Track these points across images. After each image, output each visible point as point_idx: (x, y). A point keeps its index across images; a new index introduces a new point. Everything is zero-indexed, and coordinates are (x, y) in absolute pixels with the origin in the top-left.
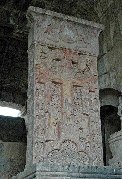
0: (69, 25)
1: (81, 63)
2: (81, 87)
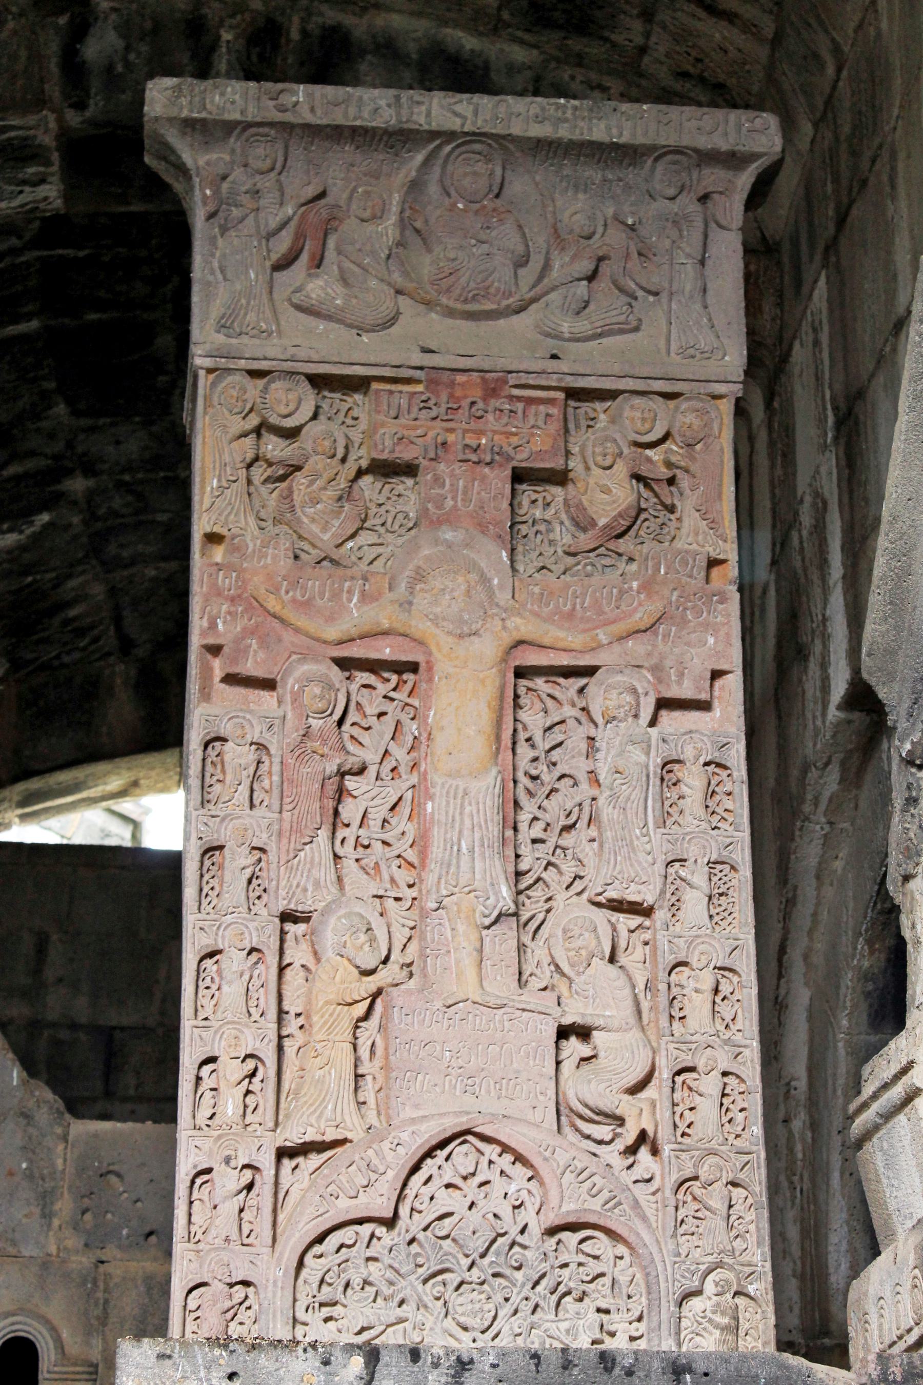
0: (481, 167)
1: (596, 471)
2: (590, 671)
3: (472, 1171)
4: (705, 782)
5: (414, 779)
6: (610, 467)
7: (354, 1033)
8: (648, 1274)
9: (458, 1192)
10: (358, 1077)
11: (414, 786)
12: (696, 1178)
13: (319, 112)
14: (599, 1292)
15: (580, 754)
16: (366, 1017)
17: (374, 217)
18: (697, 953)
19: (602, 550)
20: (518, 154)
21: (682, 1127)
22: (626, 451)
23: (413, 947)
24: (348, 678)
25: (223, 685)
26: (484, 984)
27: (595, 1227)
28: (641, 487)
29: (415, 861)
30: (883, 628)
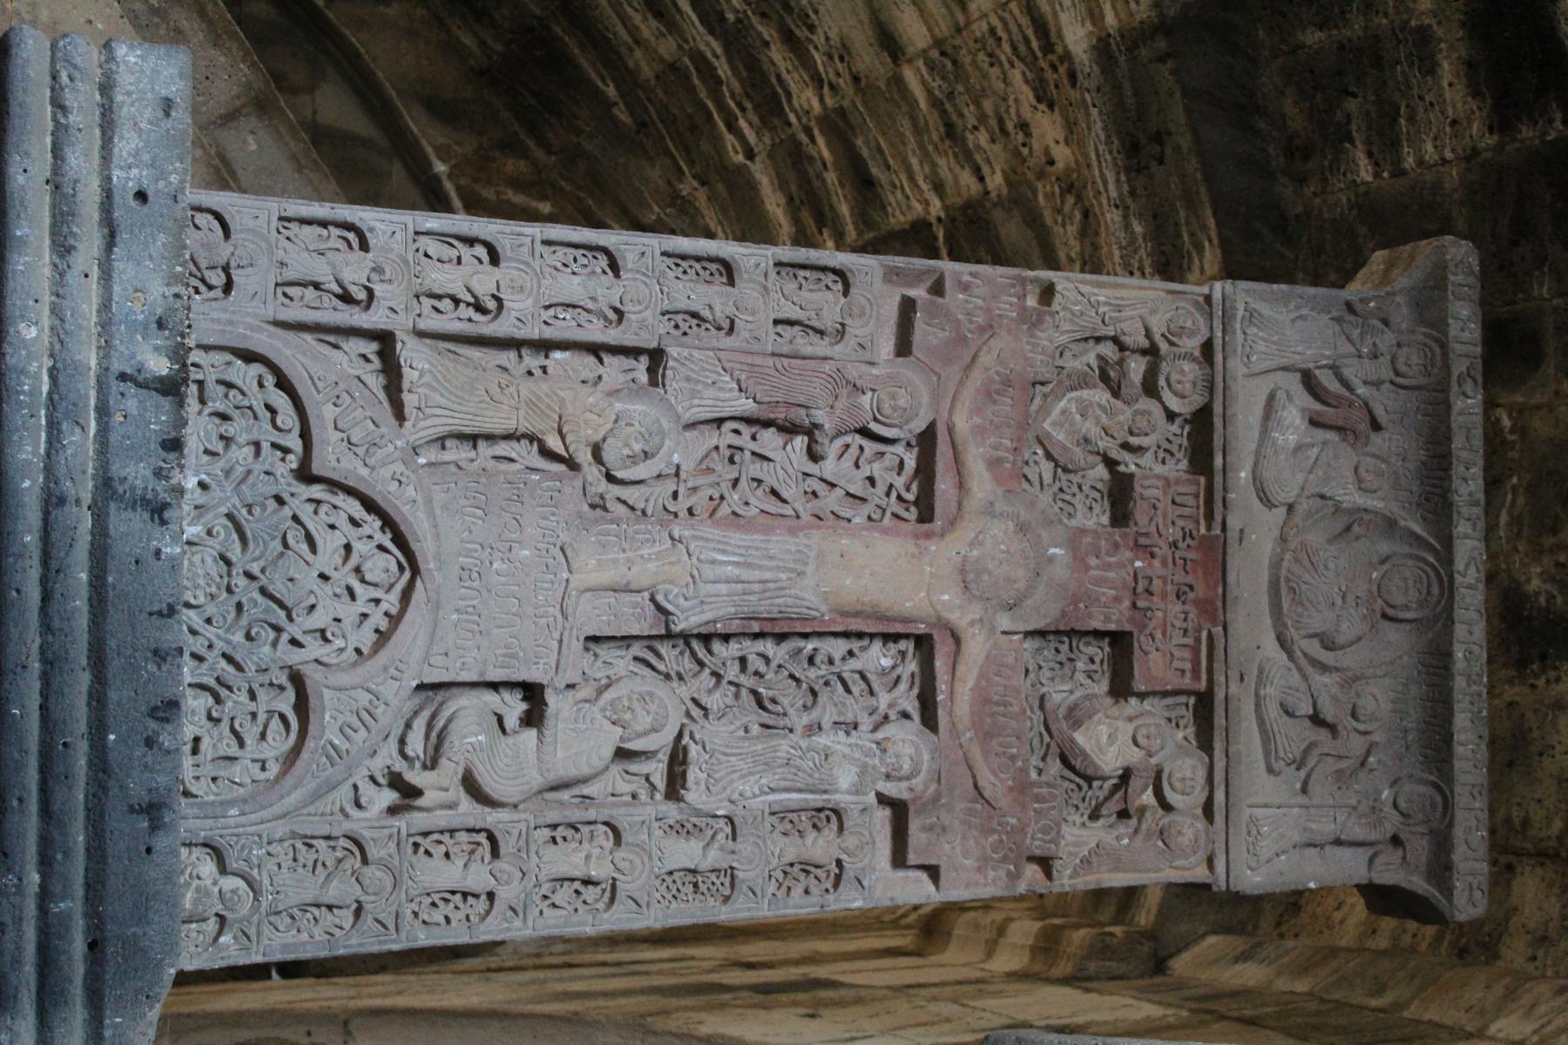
0: (1413, 595)
1: (1130, 728)
3: (368, 577)
4: (821, 862)
5: (806, 517)
6: (1136, 744)
7: (525, 436)
8: (245, 801)
9: (340, 561)
10: (473, 439)
11: (798, 517)
12: (365, 861)
13: (1461, 419)
14: (220, 740)
15: (840, 713)
16: (547, 453)
17: (1360, 481)
18: (631, 857)
19: (1047, 739)
20: (1430, 635)
21: (426, 843)
22: (1153, 761)
24: (909, 444)
25: (898, 298)
26: (588, 594)
28: (1114, 781)
29: (720, 513)
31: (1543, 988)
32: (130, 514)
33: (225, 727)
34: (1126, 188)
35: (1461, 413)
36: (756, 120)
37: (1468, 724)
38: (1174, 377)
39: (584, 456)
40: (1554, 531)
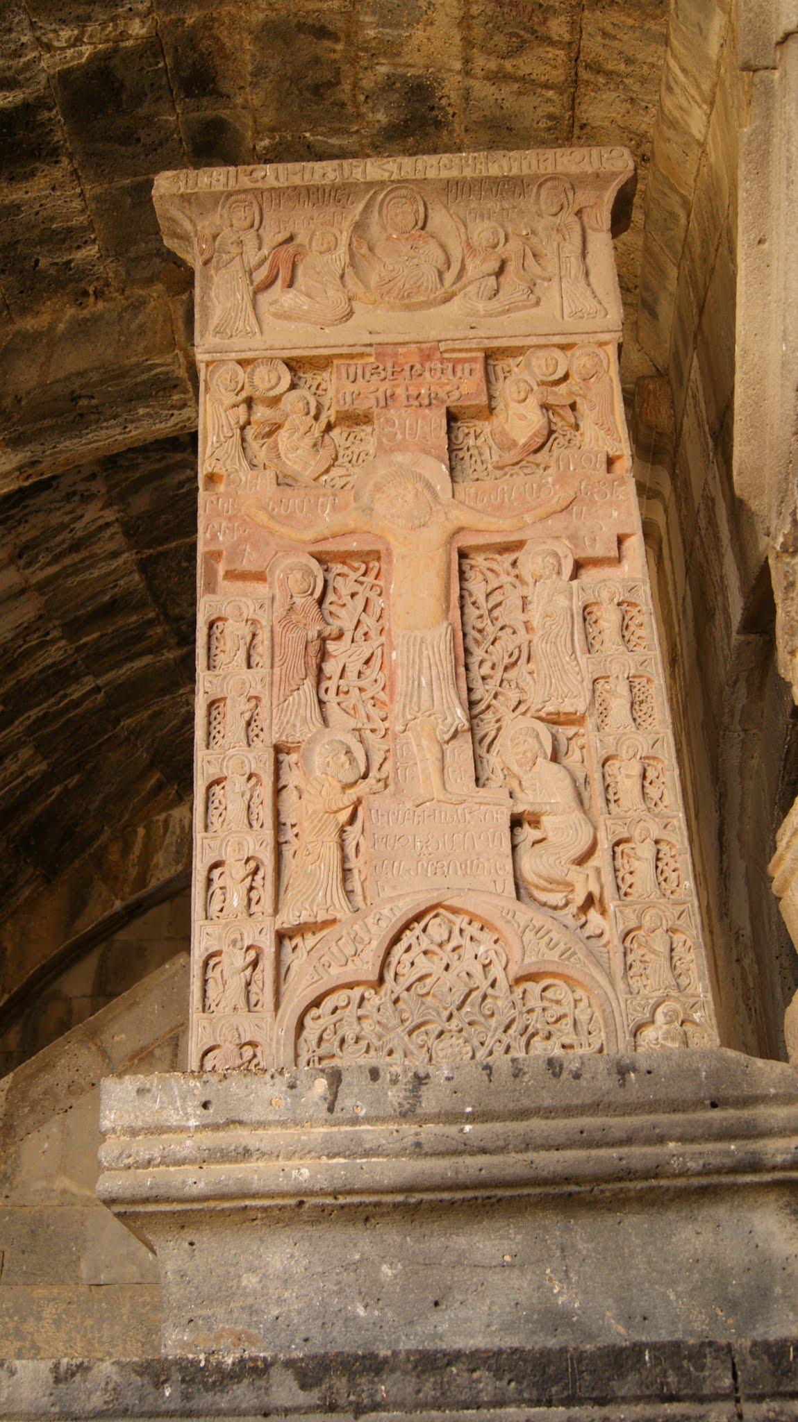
0: (407, 208)
2: (519, 545)
3: (445, 937)
4: (620, 617)
6: (524, 400)
7: (340, 836)
8: (604, 1011)
9: (435, 958)
10: (346, 872)
12: (639, 928)
13: (282, 180)
16: (352, 819)
17: (329, 249)
21: (624, 888)
22: (535, 388)
23: (388, 766)
26: (447, 786)
27: (554, 975)
30: (748, 449)
31: (669, 103)
32: (424, 1099)
33: (552, 1028)
34: (112, 422)
35: (277, 178)
36: (74, 687)
37: (496, 165)
38: (268, 386)
39: (352, 794)
40: (343, 105)
